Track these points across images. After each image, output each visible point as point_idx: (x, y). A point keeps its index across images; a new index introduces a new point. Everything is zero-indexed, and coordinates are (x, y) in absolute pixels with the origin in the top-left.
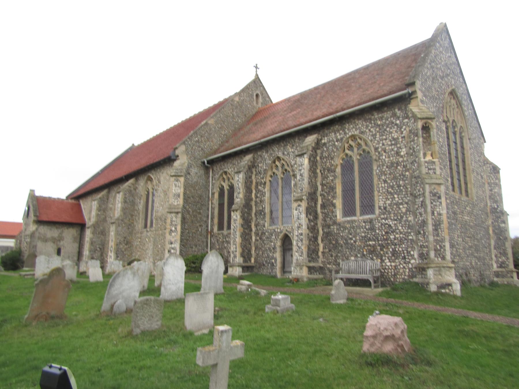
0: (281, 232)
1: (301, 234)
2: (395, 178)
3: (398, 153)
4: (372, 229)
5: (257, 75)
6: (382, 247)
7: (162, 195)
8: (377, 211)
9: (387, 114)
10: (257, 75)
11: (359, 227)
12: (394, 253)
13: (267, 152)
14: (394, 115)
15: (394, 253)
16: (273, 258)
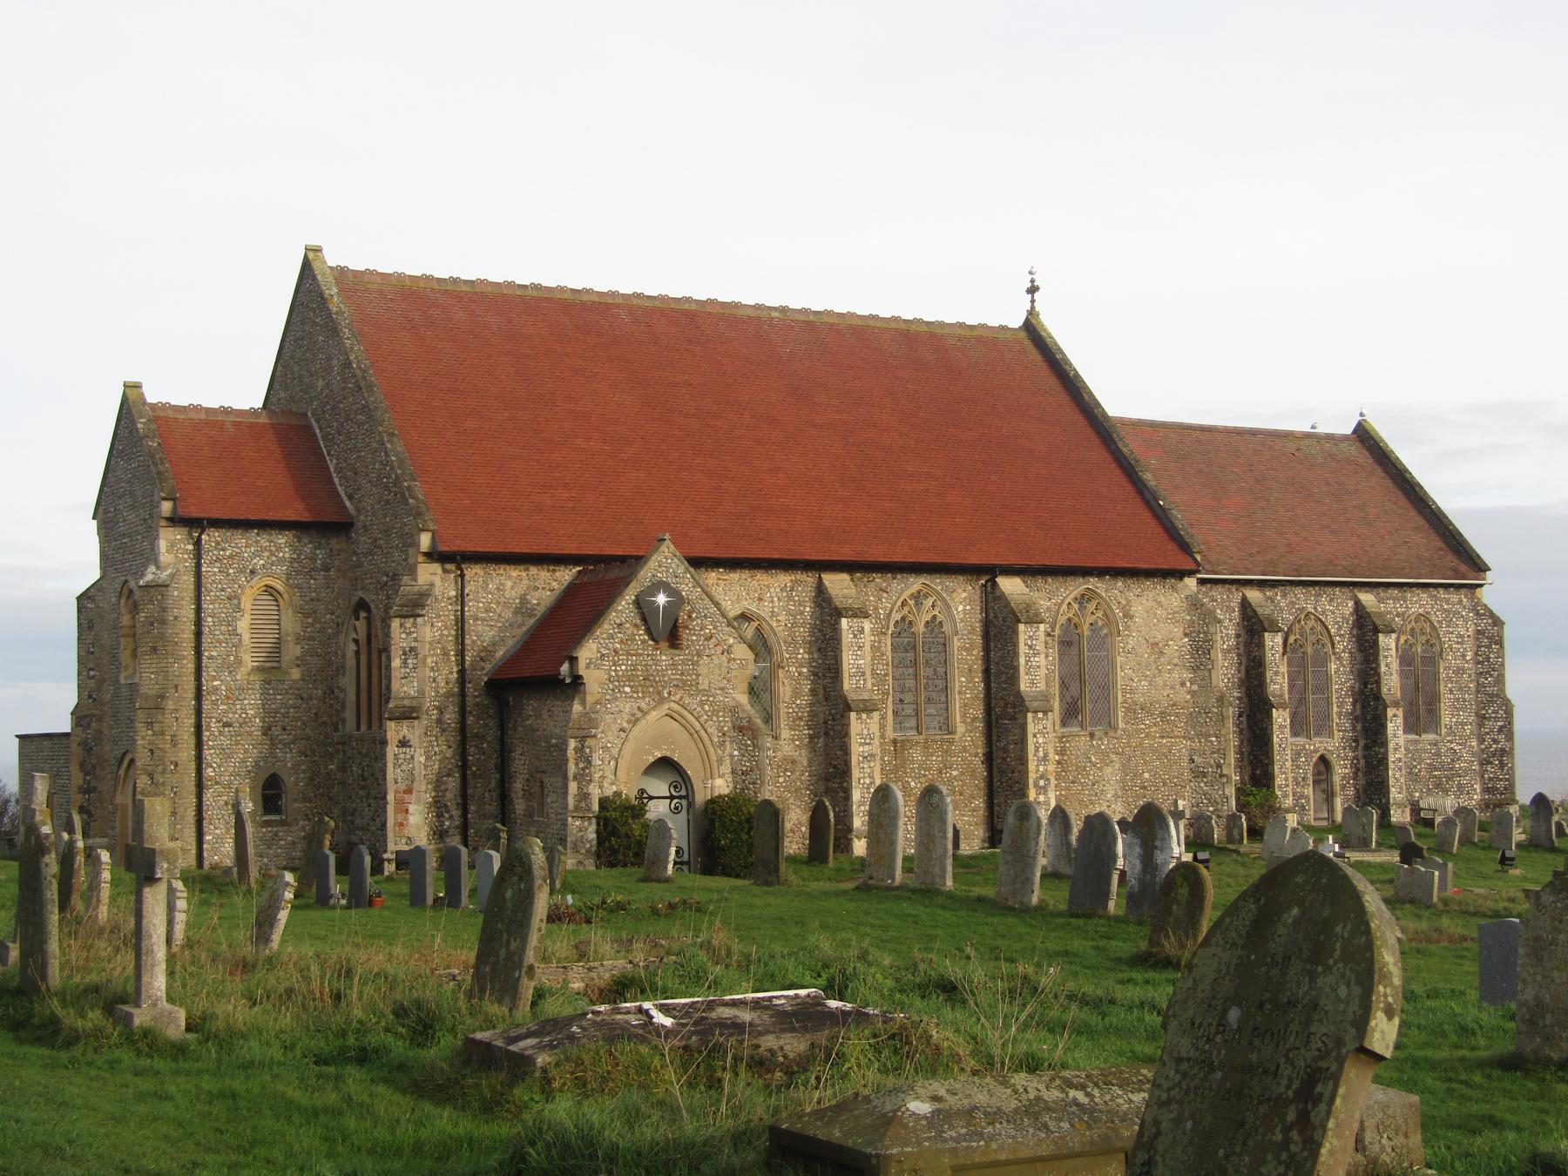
0: (1315, 751)
1: (1400, 760)
2: (1461, 689)
3: (1464, 656)
4: (1438, 754)
5: (1032, 312)
6: (1449, 778)
7: (1145, 653)
8: (1444, 731)
9: (1454, 598)
10: (1032, 312)
11: (1425, 751)
12: (1460, 787)
13: (1284, 596)
14: (1460, 602)
15: (1460, 787)
16: (1302, 796)
